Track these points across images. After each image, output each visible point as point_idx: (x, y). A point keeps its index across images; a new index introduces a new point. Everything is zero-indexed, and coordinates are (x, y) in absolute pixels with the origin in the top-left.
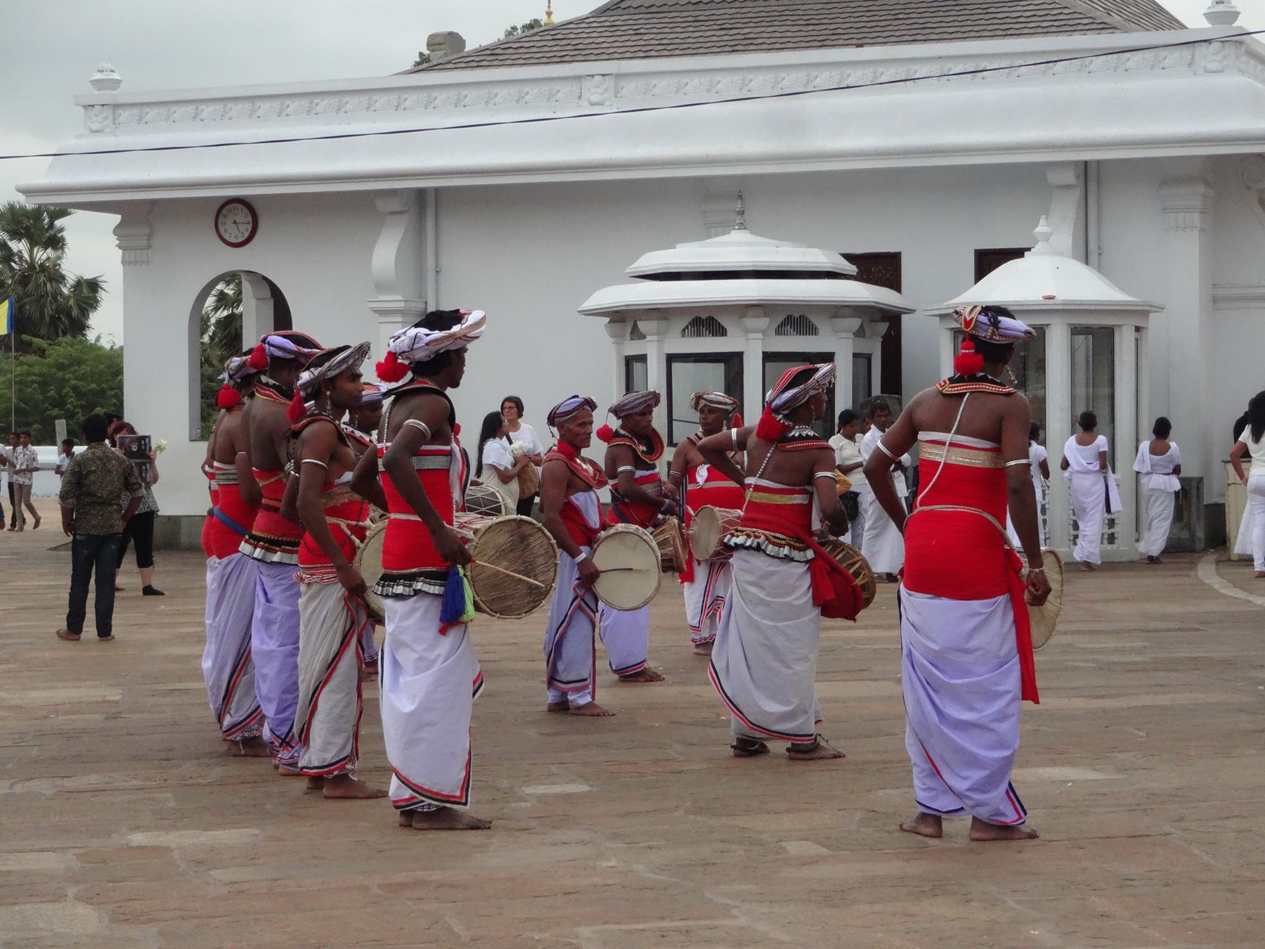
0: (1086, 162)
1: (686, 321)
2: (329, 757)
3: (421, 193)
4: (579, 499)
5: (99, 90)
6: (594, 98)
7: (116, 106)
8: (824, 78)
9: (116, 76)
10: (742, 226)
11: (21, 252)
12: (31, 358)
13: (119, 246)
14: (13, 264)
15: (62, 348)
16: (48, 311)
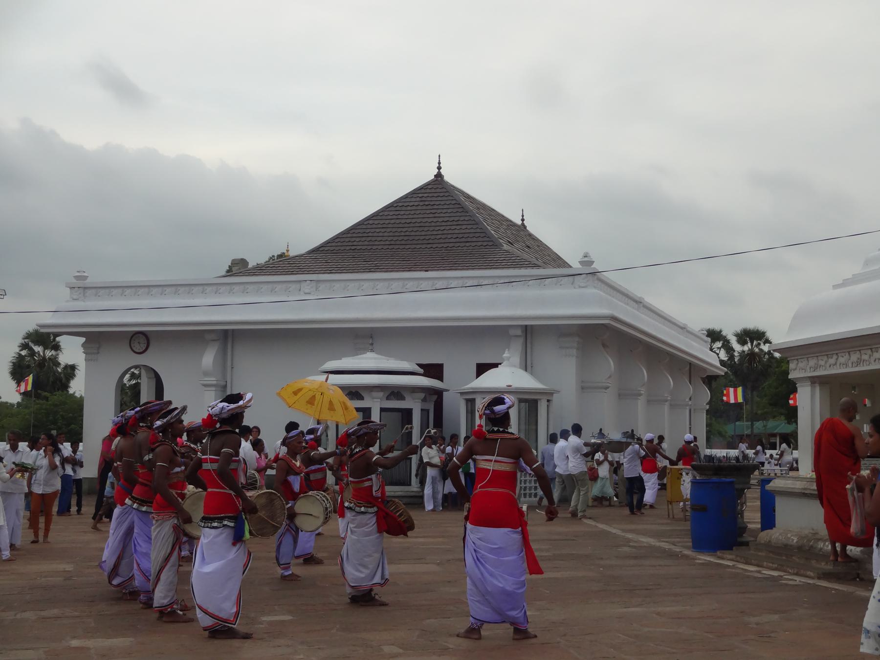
0: (526, 326)
3: (226, 332)
4: (291, 478)
5: (77, 280)
6: (307, 291)
7: (85, 288)
8: (410, 285)
9: (85, 274)
10: (372, 350)
11: (39, 352)
12: (41, 402)
13: (84, 352)
14: (35, 357)
15: (56, 397)
16: (51, 379)
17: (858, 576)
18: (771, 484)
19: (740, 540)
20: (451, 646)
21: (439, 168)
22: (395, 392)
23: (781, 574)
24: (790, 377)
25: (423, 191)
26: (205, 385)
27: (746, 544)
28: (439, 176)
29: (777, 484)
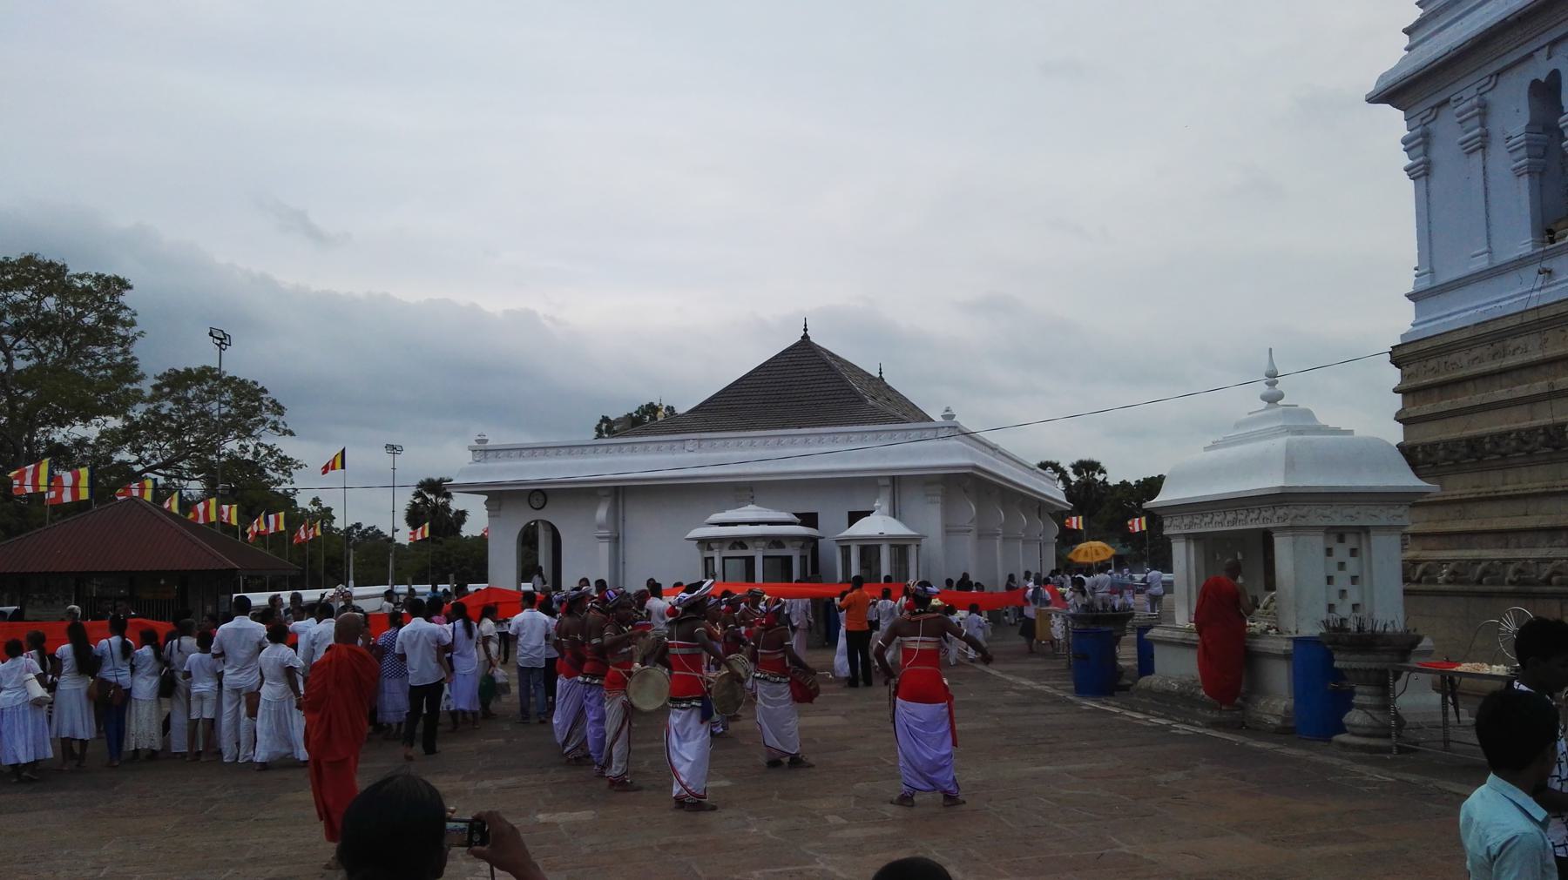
0: (894, 477)
1: (729, 545)
2: (618, 772)
6: (691, 449)
7: (486, 451)
9: (486, 438)
10: (753, 503)
17: (1244, 724)
18: (1148, 634)
19: (1120, 683)
20: (889, 815)
21: (806, 330)
22: (776, 541)
23: (1170, 722)
24: (1164, 533)
25: (791, 352)
26: (600, 538)
27: (1126, 688)
28: (805, 337)
29: (1155, 633)
